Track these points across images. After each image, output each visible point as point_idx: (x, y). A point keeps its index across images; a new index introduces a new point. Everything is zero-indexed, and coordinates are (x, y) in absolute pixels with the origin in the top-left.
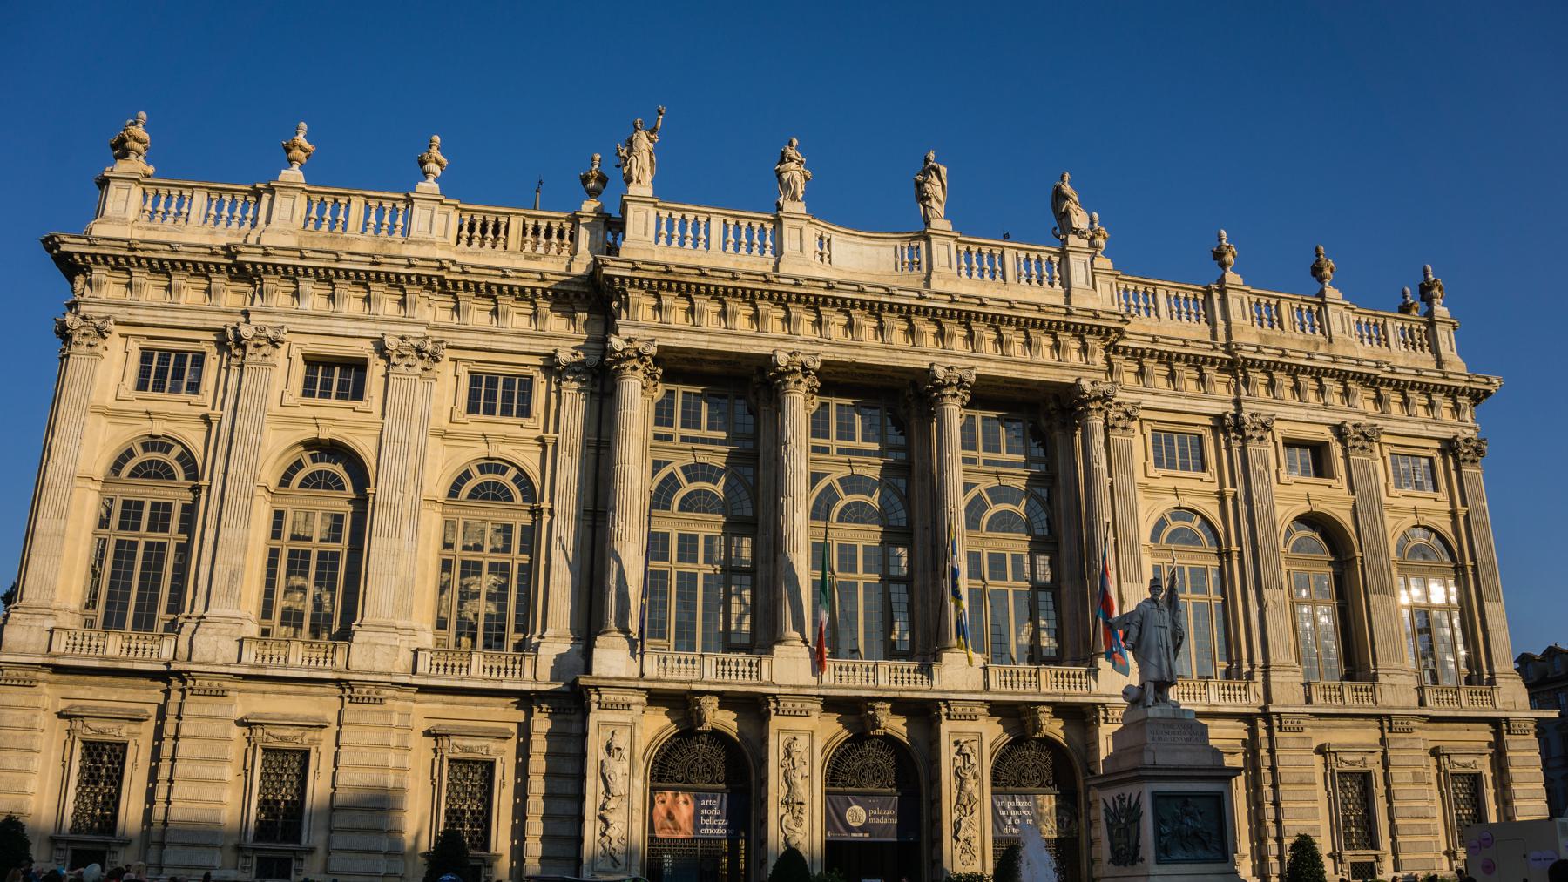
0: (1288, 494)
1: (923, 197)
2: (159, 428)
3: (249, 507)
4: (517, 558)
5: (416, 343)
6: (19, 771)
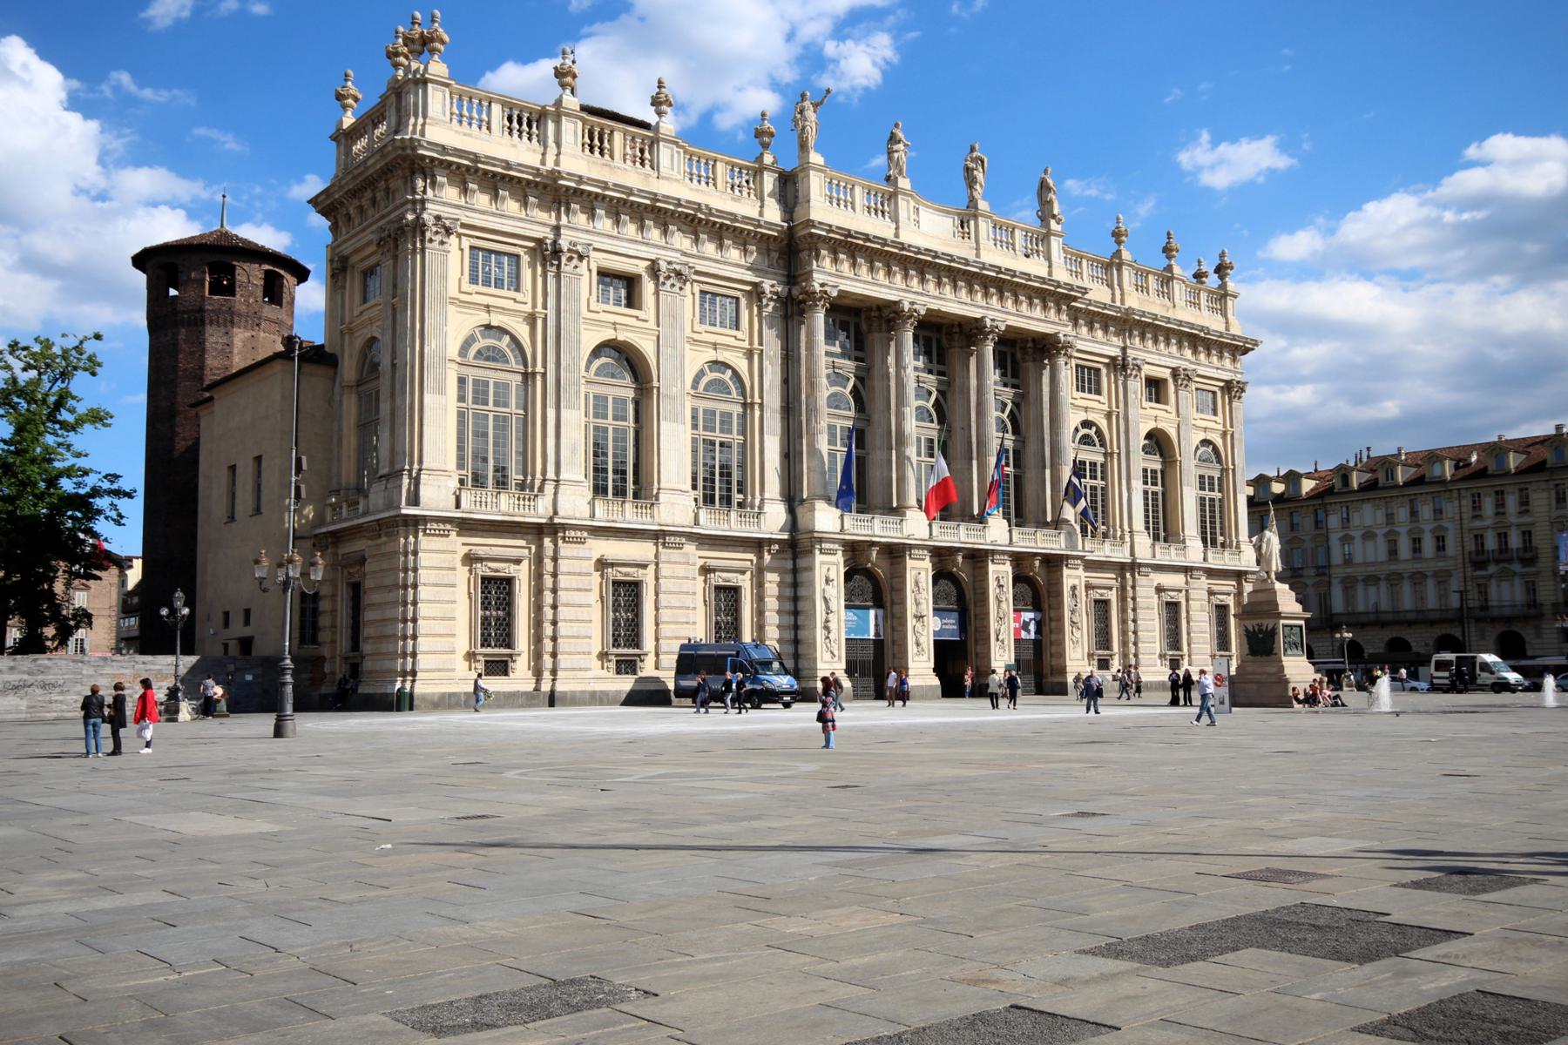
0: (1146, 417)
1: (971, 182)
2: (496, 320)
3: (578, 392)
4: (735, 438)
5: (678, 267)
6: (448, 602)
